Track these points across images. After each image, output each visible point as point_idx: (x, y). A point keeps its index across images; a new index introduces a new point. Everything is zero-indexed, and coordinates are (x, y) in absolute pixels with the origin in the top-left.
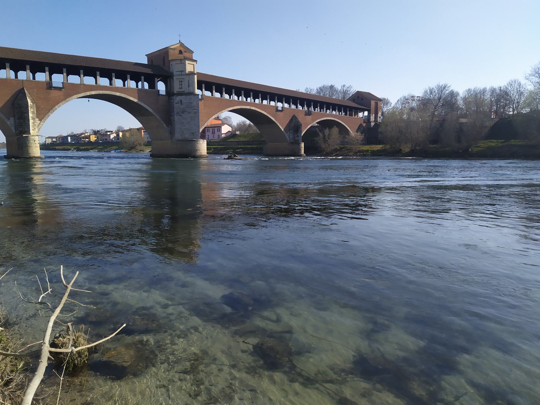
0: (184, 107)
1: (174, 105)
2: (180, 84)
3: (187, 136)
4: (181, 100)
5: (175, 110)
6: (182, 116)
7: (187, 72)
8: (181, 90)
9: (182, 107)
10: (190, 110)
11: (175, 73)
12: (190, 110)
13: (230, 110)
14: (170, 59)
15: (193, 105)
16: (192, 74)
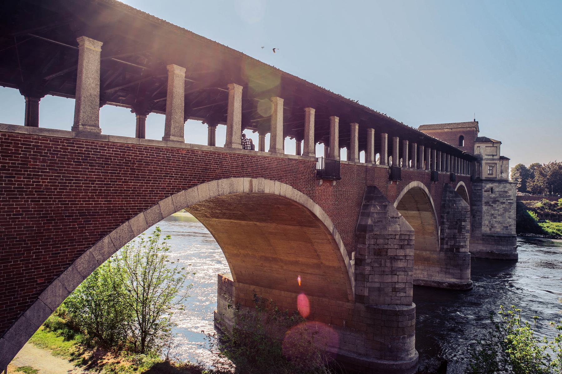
1: (482, 192)
4: (492, 189)
5: (483, 199)
9: (493, 196)
10: (504, 200)
11: (485, 157)
15: (508, 194)
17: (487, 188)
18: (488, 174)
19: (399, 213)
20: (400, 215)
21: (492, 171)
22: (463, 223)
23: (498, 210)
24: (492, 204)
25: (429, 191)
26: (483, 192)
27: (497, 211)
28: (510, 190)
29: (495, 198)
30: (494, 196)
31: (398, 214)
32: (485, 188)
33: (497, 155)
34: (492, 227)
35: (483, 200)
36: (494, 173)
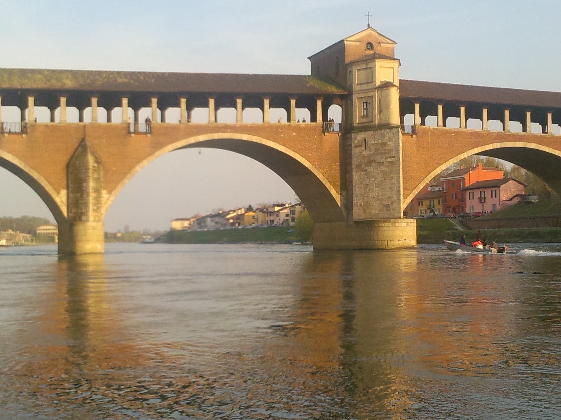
0: (371, 153)
1: (351, 150)
2: (365, 107)
3: (375, 211)
4: (365, 140)
6: (366, 170)
7: (378, 84)
9: (366, 153)
10: (382, 158)
11: (356, 88)
12: (382, 158)
13: (480, 151)
14: (348, 59)
15: (387, 148)
16: (387, 85)
17: (358, 141)
21: (367, 112)
24: (366, 168)
26: (353, 149)
28: (390, 139)
29: (369, 156)
32: (356, 142)
33: (372, 82)
35: (353, 162)
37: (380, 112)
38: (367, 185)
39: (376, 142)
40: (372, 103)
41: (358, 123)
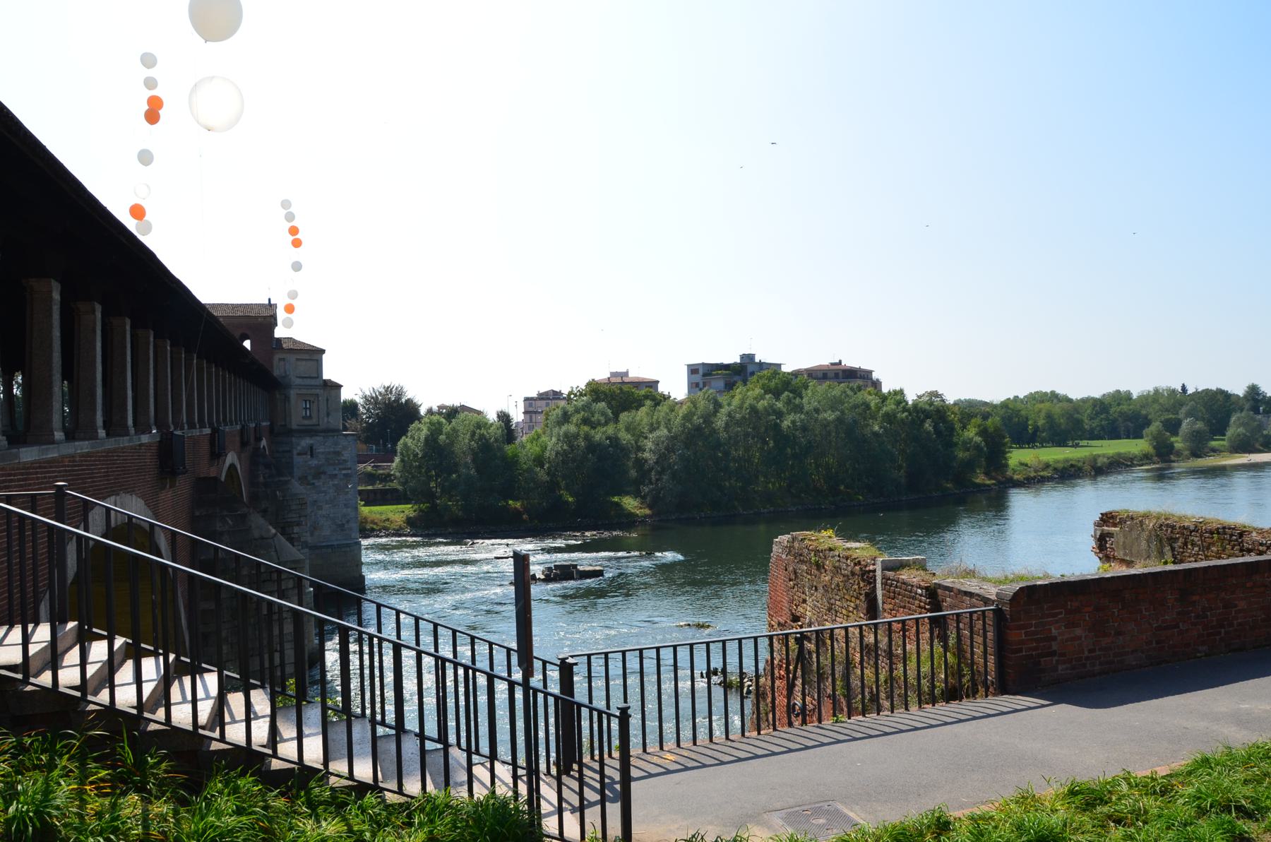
2: (304, 406)
4: (311, 448)
5: (295, 470)
8: (306, 422)
9: (314, 462)
10: (335, 469)
15: (343, 458)
18: (303, 418)
19: (271, 527)
20: (273, 531)
21: (310, 412)
22: (296, 529)
23: (325, 492)
25: (241, 467)
26: (295, 456)
27: (323, 494)
28: (345, 448)
30: (316, 462)
31: (269, 531)
32: (299, 448)
33: (318, 377)
34: (315, 528)
36: (314, 415)
37: (328, 415)
38: (316, 501)
39: (327, 450)
40: (318, 405)
41: (298, 425)
